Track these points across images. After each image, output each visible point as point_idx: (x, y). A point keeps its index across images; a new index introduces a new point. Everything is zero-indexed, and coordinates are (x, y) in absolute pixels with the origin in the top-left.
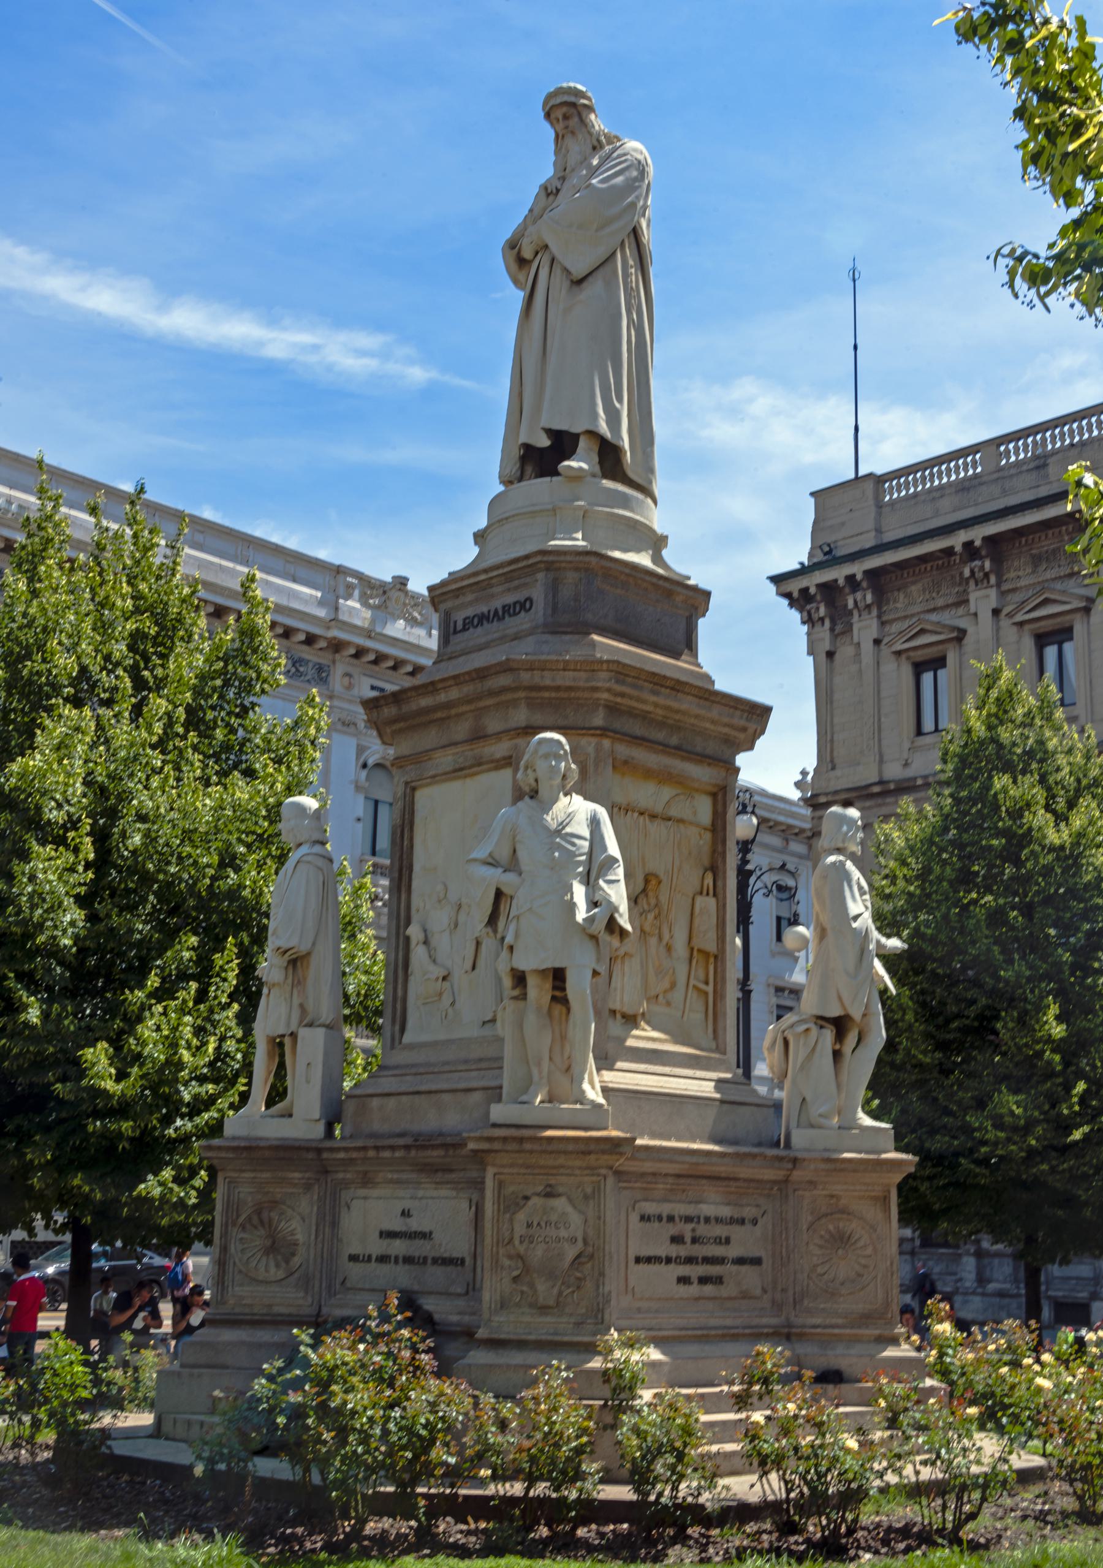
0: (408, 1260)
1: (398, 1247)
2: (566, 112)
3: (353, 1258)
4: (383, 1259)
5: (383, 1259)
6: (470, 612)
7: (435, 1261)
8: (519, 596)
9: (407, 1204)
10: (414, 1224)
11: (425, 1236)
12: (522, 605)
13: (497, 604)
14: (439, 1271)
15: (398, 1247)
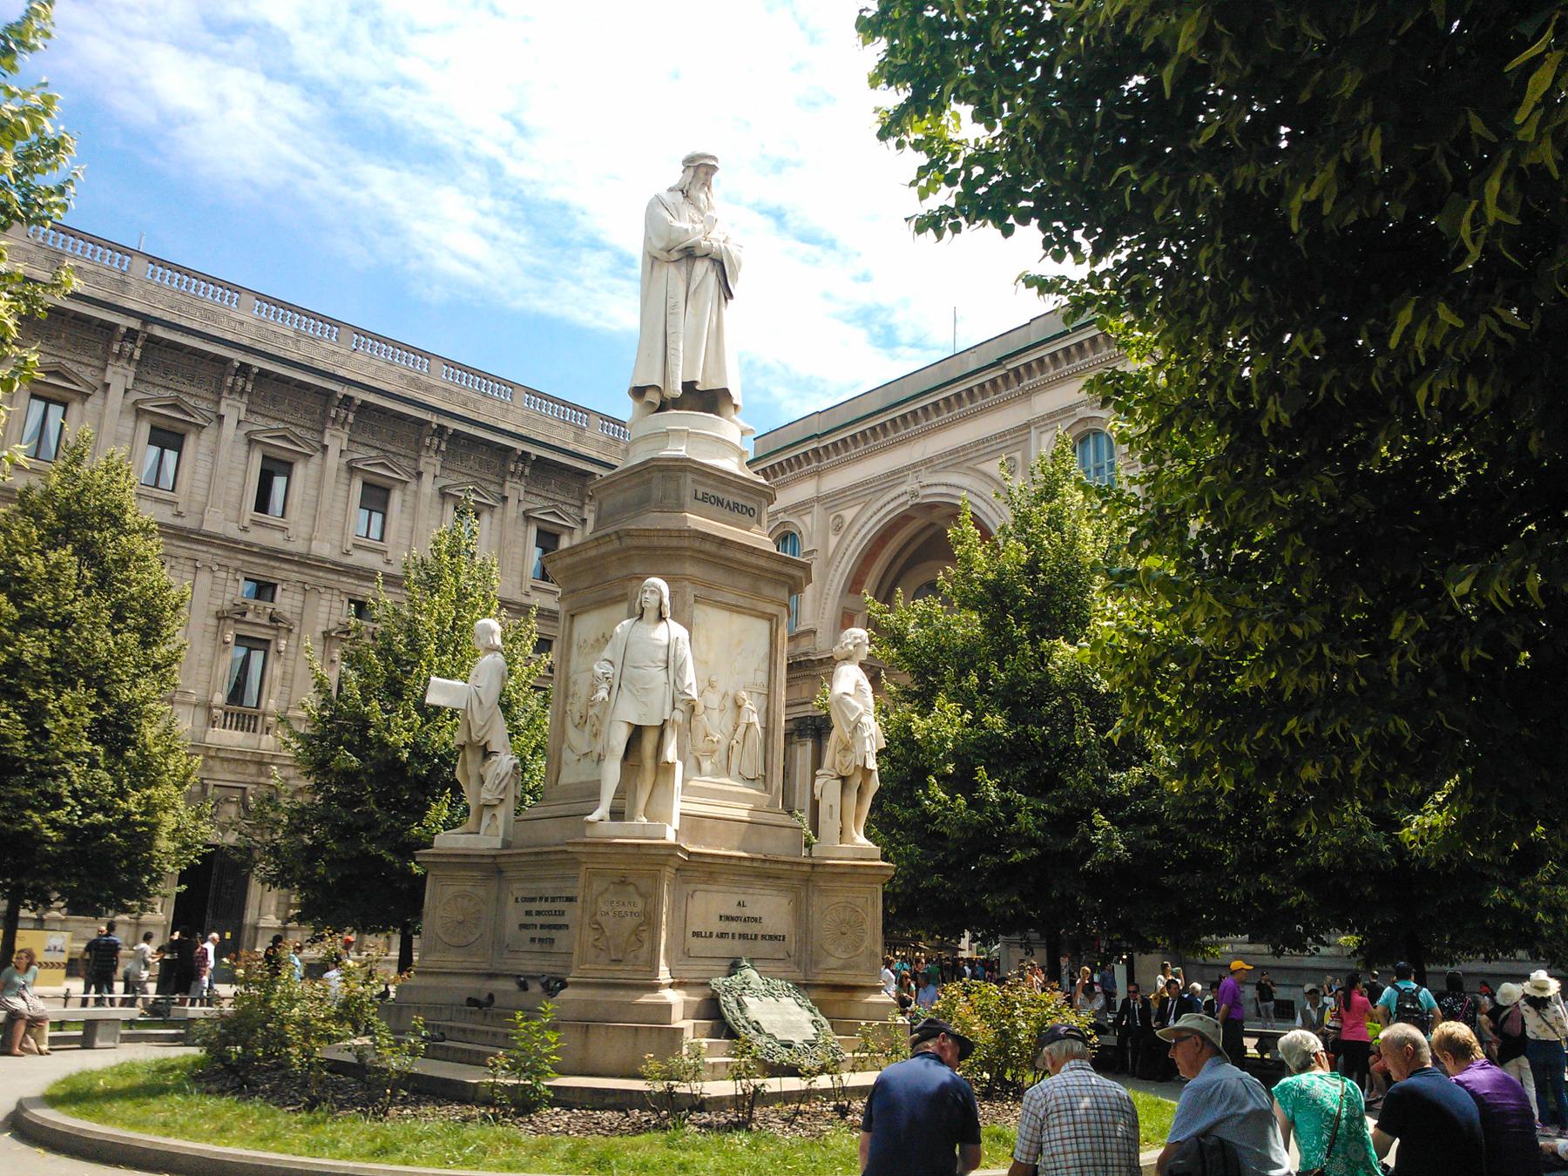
0: (743, 936)
1: (735, 927)
2: (700, 169)
3: (696, 934)
4: (722, 935)
5: (722, 935)
6: (708, 490)
7: (763, 937)
8: (749, 504)
9: (742, 898)
10: (747, 912)
11: (755, 920)
12: (748, 511)
13: (732, 499)
14: (766, 943)
15: (735, 927)
